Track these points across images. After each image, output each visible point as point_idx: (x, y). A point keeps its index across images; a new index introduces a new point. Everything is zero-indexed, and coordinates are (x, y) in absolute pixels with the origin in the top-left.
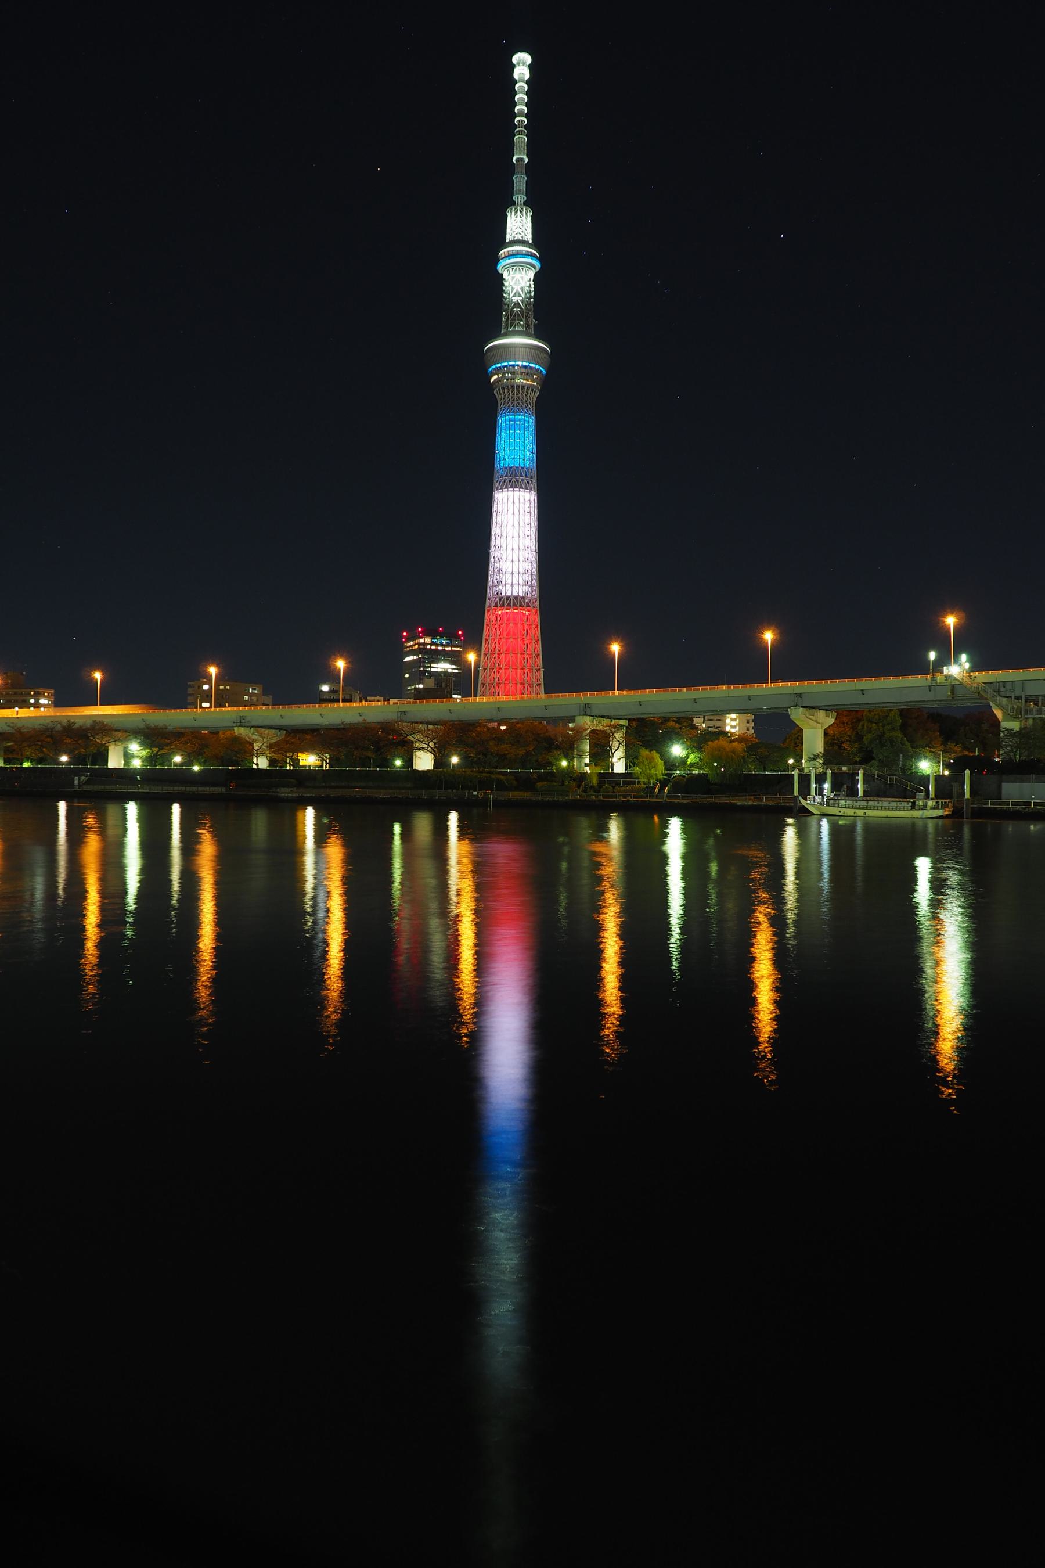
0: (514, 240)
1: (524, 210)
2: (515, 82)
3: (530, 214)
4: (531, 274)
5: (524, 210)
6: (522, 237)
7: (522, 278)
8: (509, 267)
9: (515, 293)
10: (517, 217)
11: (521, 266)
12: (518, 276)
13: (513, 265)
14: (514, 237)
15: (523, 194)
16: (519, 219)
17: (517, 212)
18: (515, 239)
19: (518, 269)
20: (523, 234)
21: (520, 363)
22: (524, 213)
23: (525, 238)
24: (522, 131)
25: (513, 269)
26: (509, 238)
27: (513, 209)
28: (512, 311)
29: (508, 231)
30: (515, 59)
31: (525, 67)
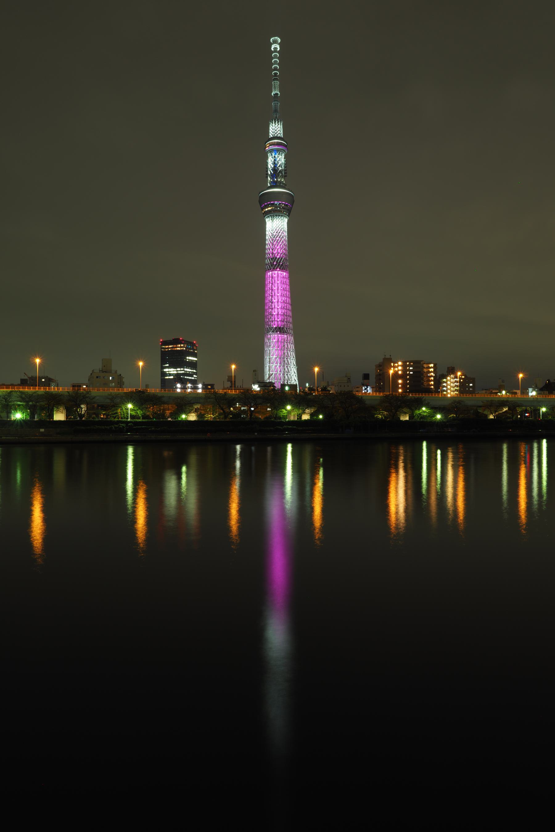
2: (273, 52)
4: (283, 155)
5: (279, 120)
8: (272, 151)
10: (276, 124)
14: (275, 135)
15: (278, 112)
17: (276, 121)
18: (275, 136)
21: (276, 202)
23: (279, 135)
24: (276, 78)
26: (271, 136)
29: (270, 131)
30: (271, 39)
31: (278, 45)
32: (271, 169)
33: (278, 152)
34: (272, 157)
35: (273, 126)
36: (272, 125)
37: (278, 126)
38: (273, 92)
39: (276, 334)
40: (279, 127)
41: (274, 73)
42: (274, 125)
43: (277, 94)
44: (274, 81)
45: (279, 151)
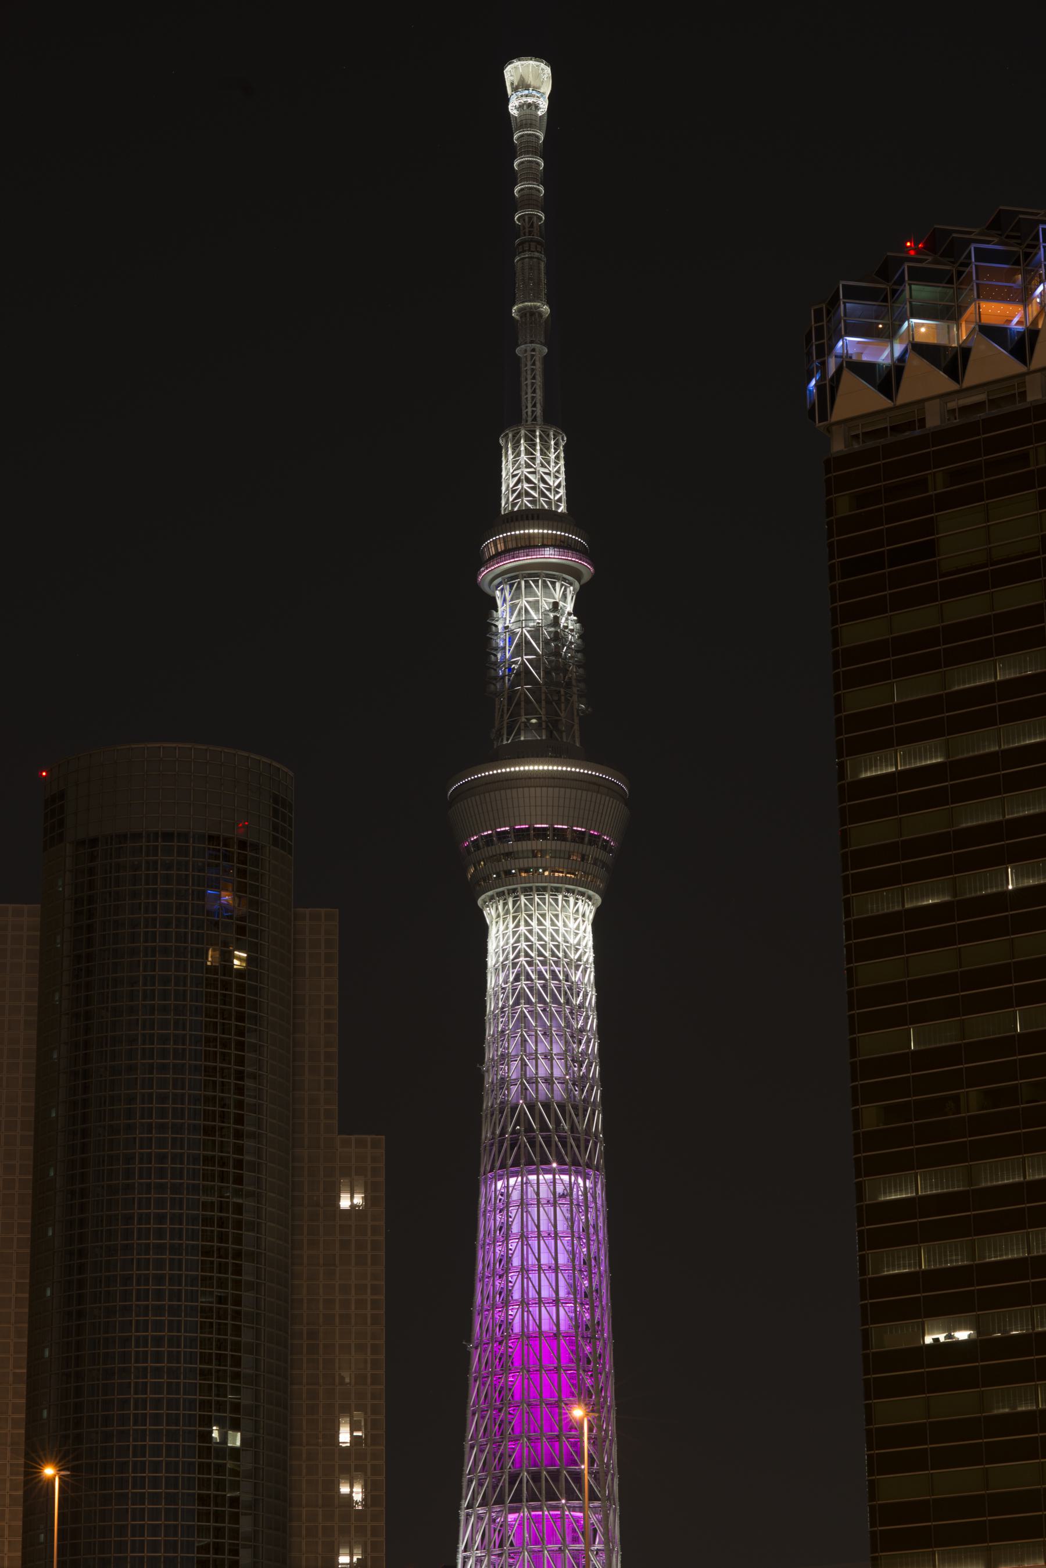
0: (512, 512)
1: (538, 433)
6: (532, 502)
7: (535, 605)
9: (518, 645)
10: (519, 455)
11: (530, 575)
12: (523, 602)
13: (512, 577)
14: (514, 505)
16: (523, 458)
17: (519, 441)
18: (516, 509)
19: (523, 583)
20: (537, 496)
22: (538, 440)
25: (511, 586)
27: (510, 435)
28: (512, 694)
29: (504, 489)
41: (518, 219)
44: (524, 251)
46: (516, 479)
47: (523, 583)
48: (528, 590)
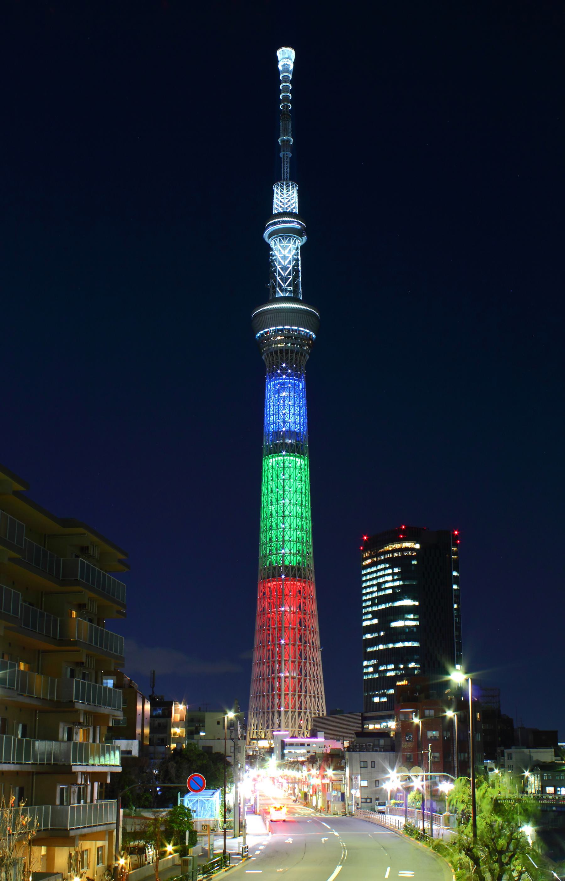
3: (295, 190)
5: (295, 185)
10: (289, 191)
14: (287, 209)
17: (289, 186)
18: (288, 211)
27: (285, 183)
32: (280, 267)
33: (293, 239)
34: (282, 247)
35: (283, 194)
36: (281, 191)
37: (292, 195)
38: (281, 135)
39: (292, 581)
40: (293, 197)
42: (285, 191)
43: (288, 141)
45: (295, 237)
46: (288, 200)
47: (291, 239)
48: (281, 242)
